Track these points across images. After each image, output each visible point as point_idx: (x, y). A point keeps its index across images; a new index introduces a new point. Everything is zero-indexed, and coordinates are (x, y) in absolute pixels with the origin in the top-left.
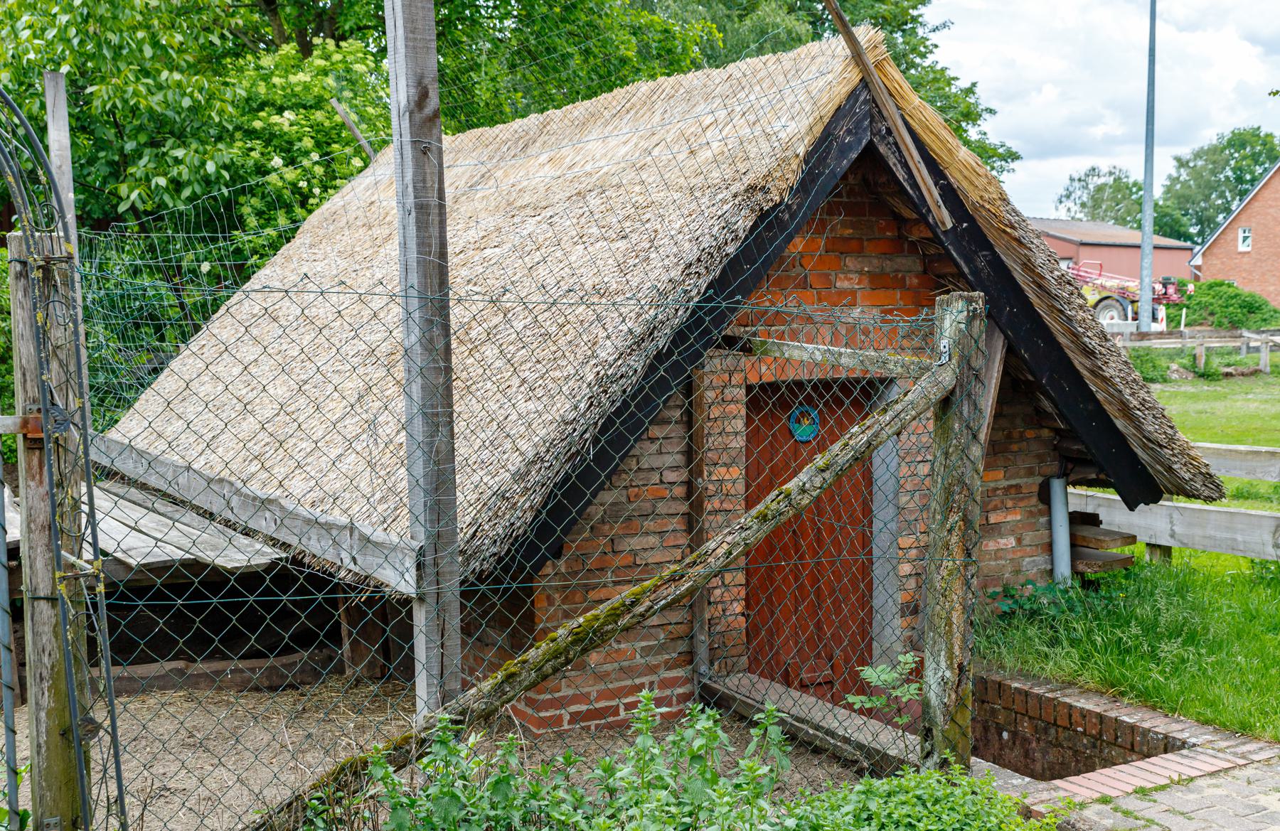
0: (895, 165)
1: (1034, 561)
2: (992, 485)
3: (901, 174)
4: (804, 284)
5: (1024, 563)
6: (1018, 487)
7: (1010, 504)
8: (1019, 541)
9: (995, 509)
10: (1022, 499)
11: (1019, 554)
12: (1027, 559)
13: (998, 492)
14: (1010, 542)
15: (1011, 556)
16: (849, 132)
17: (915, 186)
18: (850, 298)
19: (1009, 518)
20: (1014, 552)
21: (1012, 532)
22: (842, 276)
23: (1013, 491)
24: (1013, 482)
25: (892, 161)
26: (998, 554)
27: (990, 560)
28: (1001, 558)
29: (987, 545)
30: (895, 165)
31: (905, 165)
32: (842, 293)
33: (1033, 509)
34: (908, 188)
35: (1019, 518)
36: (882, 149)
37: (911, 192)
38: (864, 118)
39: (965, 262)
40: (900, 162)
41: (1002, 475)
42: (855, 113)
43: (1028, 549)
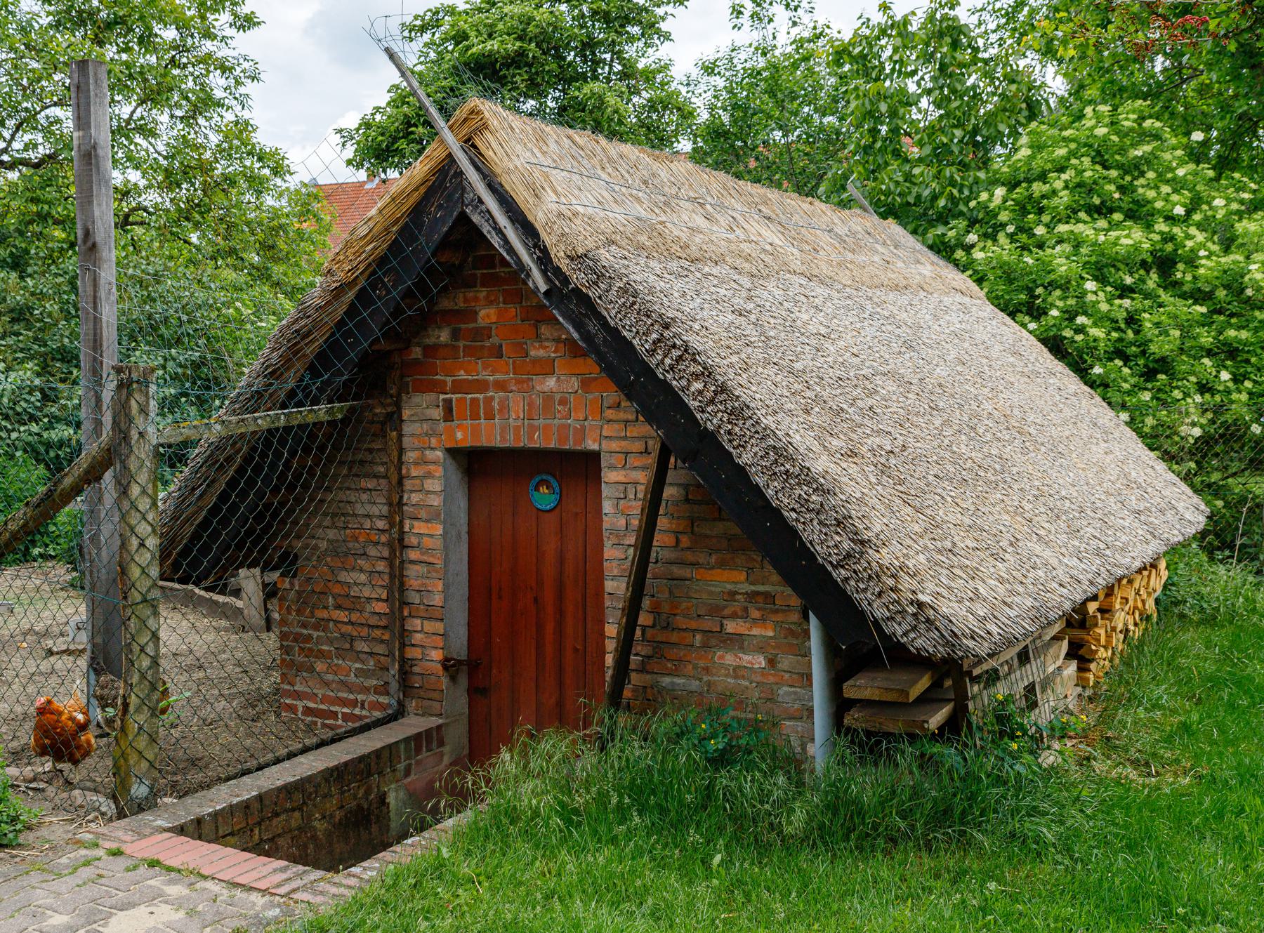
0: (489, 232)
1: (795, 693)
2: (729, 587)
3: (495, 241)
4: (498, 352)
5: (780, 692)
6: (769, 598)
7: (756, 614)
8: (772, 662)
9: (734, 616)
10: (777, 611)
11: (772, 680)
12: (785, 688)
13: (738, 597)
14: (760, 661)
15: (759, 679)
16: (440, 207)
17: (511, 250)
18: (547, 368)
19: (755, 632)
20: (763, 675)
21: (761, 650)
22: (537, 345)
23: (760, 599)
24: (761, 588)
25: (486, 229)
26: (737, 671)
27: (726, 676)
28: (743, 678)
29: (722, 657)
30: (489, 232)
31: (499, 231)
32: (536, 361)
33: (793, 627)
34: (505, 254)
35: (771, 634)
36: (476, 218)
37: (508, 258)
38: (455, 190)
39: (574, 327)
40: (495, 229)
41: (743, 576)
42: (446, 188)
43: (787, 676)
